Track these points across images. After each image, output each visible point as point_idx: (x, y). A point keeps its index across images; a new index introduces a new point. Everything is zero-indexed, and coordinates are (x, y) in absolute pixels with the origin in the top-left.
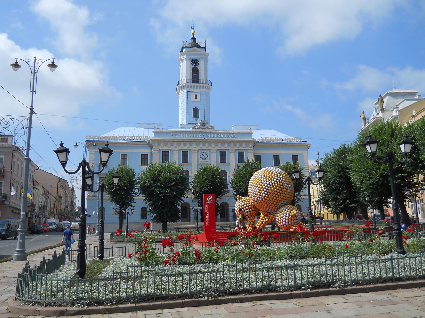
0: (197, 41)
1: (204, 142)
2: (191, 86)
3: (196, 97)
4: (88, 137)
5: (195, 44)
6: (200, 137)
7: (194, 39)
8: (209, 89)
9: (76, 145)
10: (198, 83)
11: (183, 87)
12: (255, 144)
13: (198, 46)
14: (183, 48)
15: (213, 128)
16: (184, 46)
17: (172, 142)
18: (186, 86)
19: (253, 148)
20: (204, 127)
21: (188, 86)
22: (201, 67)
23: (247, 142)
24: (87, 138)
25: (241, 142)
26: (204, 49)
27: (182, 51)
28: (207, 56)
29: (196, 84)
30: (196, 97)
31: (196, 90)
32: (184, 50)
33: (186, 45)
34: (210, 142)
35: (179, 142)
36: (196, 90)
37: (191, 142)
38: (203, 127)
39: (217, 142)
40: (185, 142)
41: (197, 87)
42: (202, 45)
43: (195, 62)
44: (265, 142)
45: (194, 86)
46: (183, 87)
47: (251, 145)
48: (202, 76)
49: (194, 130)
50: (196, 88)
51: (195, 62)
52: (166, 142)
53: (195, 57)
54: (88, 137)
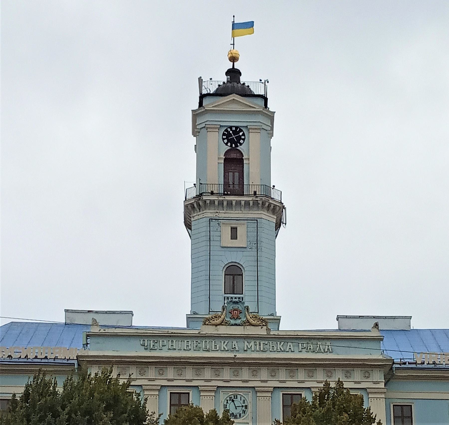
0: (243, 79)
1: (236, 364)
2: (221, 203)
3: (234, 235)
6: (225, 350)
7: (234, 74)
12: (391, 372)
13: (246, 93)
14: (202, 97)
16: (204, 92)
19: (382, 385)
20: (238, 322)
21: (212, 202)
22: (250, 148)
23: (366, 366)
25: (348, 366)
26: (262, 102)
27: (201, 104)
28: (271, 116)
30: (234, 235)
32: (206, 102)
34: (255, 365)
35: (162, 364)
36: (234, 214)
37: (199, 364)
38: (233, 322)
39: (273, 365)
41: (239, 203)
42: (258, 90)
43: (234, 136)
44: (425, 366)
45: (230, 204)
46: (199, 205)
47: (378, 376)
49: (209, 330)
51: (234, 136)
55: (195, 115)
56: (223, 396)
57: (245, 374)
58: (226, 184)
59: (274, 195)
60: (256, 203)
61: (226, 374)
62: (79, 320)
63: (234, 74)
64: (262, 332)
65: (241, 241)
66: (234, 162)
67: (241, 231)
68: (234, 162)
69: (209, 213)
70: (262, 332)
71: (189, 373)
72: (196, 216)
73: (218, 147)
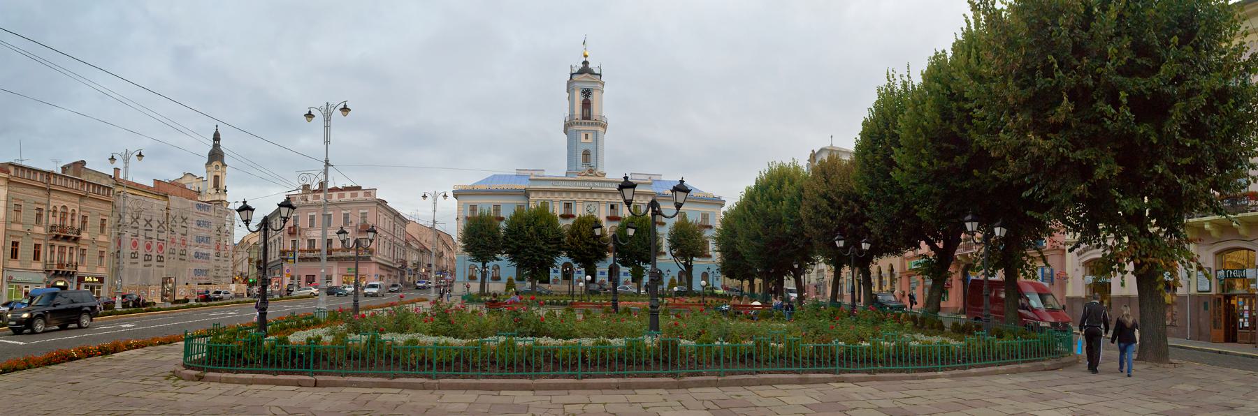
1: (591, 192)
5: (585, 69)
7: (585, 63)
9: (425, 197)
13: (591, 72)
15: (604, 175)
17: (552, 191)
22: (594, 98)
28: (603, 84)
32: (575, 78)
33: (576, 70)
35: (560, 191)
40: (568, 191)
42: (597, 71)
43: (587, 93)
48: (595, 111)
51: (587, 93)
52: (545, 191)
53: (588, 86)
55: (569, 84)
56: (586, 205)
57: (595, 196)
61: (588, 196)
62: (522, 173)
63: (585, 63)
66: (587, 105)
68: (587, 105)
69: (576, 128)
71: (572, 195)
72: (570, 129)
73: (579, 98)
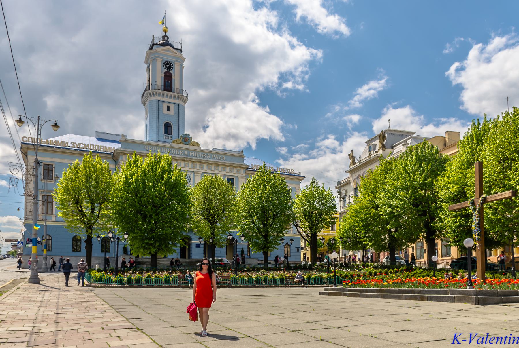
3: (168, 109)
4: (25, 139)
8: (185, 101)
10: (171, 91)
11: (153, 94)
18: (156, 93)
19: (244, 175)
21: (160, 94)
24: (23, 140)
29: (169, 93)
30: (168, 109)
31: (168, 100)
36: (168, 100)
46: (153, 94)
47: (242, 171)
48: (176, 84)
50: (168, 98)
54: (25, 139)
58: (165, 86)
59: (185, 94)
60: (178, 97)
64: (196, 148)
65: (172, 112)
67: (172, 107)
69: (159, 98)
70: (196, 148)
